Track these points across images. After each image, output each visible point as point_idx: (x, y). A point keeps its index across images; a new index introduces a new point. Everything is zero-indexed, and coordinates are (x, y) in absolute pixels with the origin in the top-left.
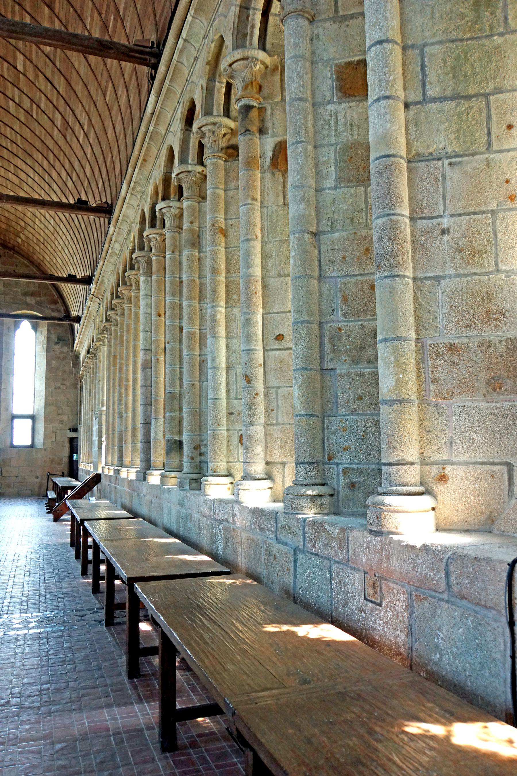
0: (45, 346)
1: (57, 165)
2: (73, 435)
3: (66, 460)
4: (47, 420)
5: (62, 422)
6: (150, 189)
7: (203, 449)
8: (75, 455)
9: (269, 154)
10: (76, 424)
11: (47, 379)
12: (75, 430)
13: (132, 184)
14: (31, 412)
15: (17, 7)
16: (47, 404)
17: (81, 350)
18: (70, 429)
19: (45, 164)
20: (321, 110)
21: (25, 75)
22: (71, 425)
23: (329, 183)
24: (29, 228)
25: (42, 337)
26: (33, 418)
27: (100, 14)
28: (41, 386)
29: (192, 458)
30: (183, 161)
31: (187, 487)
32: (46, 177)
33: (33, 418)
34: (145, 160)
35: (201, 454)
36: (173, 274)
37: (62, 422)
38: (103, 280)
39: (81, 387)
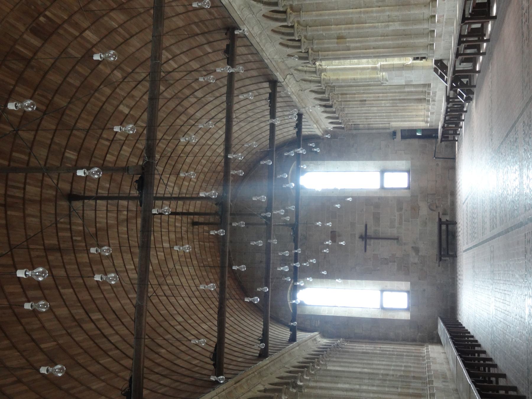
0: (319, 162)
1: (186, 103)
2: (399, 135)
3: (422, 142)
4: (385, 157)
8: (418, 134)
11: (349, 160)
12: (394, 133)
14: (378, 174)
15: (96, 94)
16: (371, 159)
17: (323, 126)
18: (394, 139)
19: (184, 118)
21: (131, 109)
25: (312, 165)
26: (383, 172)
27: (113, 9)
28: (354, 165)
32: (192, 122)
33: (383, 172)
39: (356, 127)
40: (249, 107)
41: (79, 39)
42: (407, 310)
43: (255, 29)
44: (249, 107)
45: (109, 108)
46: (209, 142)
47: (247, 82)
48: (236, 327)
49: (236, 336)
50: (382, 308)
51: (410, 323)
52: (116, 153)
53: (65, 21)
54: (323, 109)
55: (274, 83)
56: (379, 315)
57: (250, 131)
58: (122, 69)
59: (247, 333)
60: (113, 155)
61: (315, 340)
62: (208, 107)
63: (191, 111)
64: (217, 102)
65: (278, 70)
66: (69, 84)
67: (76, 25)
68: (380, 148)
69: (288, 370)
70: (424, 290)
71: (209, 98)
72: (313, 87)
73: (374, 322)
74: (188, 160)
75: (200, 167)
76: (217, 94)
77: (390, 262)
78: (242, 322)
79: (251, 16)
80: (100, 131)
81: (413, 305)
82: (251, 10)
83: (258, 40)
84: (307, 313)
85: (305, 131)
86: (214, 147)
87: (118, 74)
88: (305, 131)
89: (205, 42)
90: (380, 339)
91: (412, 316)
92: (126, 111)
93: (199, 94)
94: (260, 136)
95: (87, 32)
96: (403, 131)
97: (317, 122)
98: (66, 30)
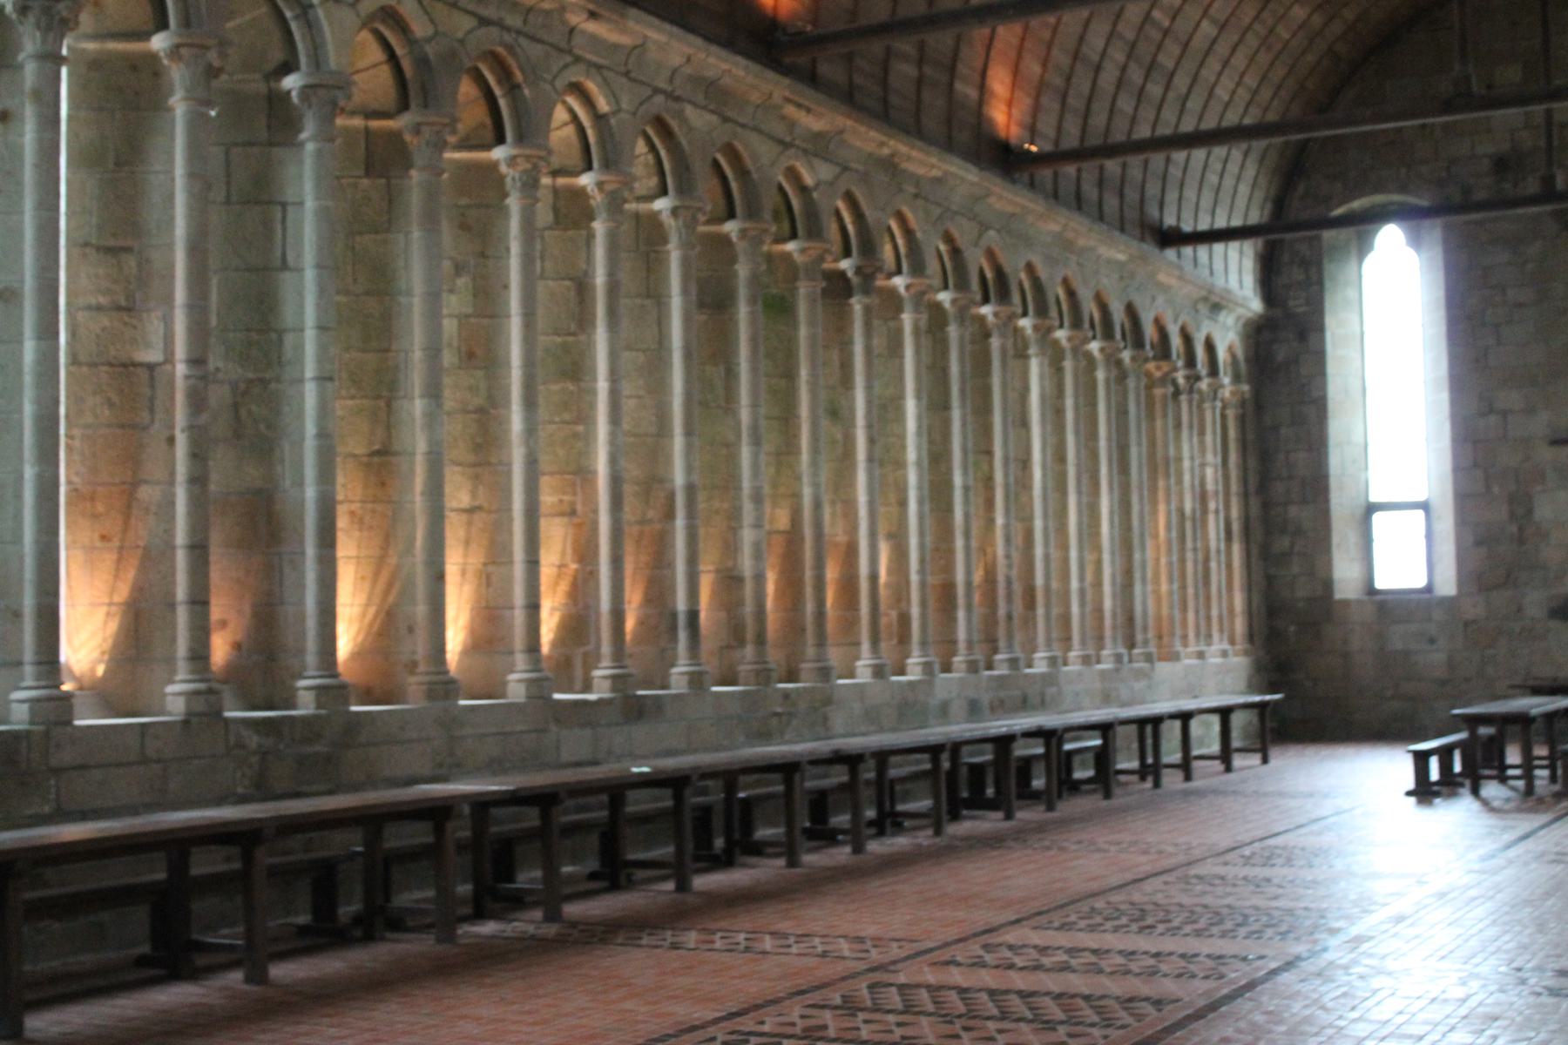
42: (1371, 591)
48: (1172, 49)
49: (1118, 54)
50: (1371, 509)
51: (1323, 601)
56: (1341, 503)
59: (1154, 89)
61: (1216, 308)
69: (962, 241)
70: (1432, 641)
73: (1316, 486)
77: (1520, 529)
78: (1214, 65)
81: (1388, 607)
84: (1329, 268)
90: (1266, 506)
91: (1345, 603)
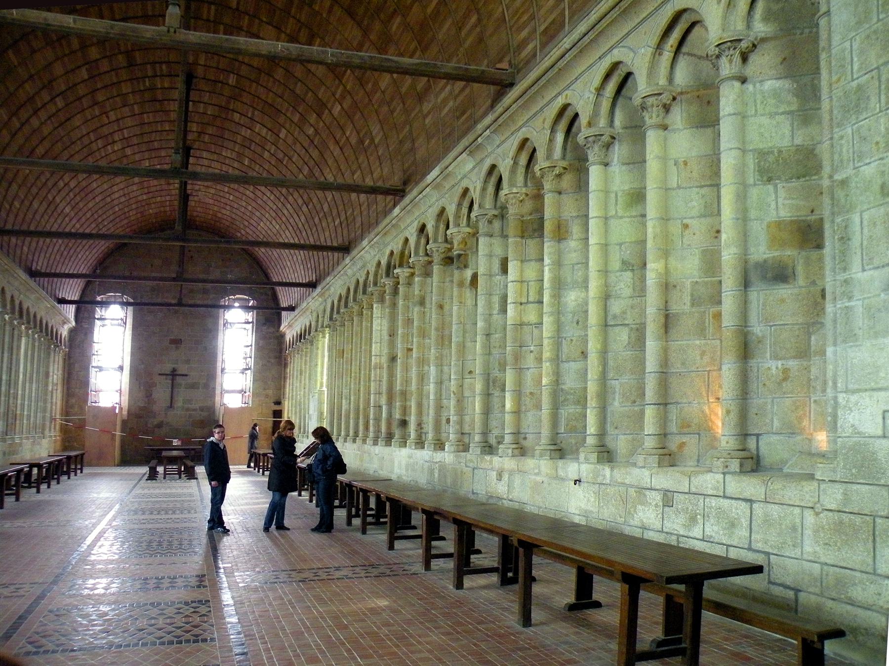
2: (277, 408)
5: (267, 396)
6: (388, 252)
7: (423, 426)
9: (469, 279)
10: (280, 398)
12: (278, 403)
13: (372, 243)
15: (291, 108)
17: (288, 332)
20: (493, 278)
22: (273, 400)
23: (495, 312)
24: (252, 227)
29: (416, 431)
30: (416, 253)
31: (414, 447)
34: (385, 234)
35: (421, 428)
36: (403, 314)
37: (267, 396)
38: (329, 287)
39: (286, 365)
40: (299, 258)
41: (333, 98)
43: (349, 270)
44: (299, 258)
45: (281, 120)
46: (267, 215)
47: (316, 259)
52: (242, 122)
53: (345, 87)
54: (299, 332)
55: (312, 285)
57: (282, 257)
58: (315, 135)
60: (240, 119)
62: (295, 216)
63: (290, 198)
64: (300, 226)
65: (323, 291)
66: (296, 84)
67: (343, 97)
68: (265, 389)
71: (303, 218)
72: (313, 324)
74: (248, 192)
75: (244, 204)
76: (306, 226)
79: (358, 267)
80: (259, 108)
82: (362, 268)
83: (342, 272)
85: (284, 313)
86: (264, 219)
87: (311, 131)
88: (284, 313)
89: (342, 220)
92: (282, 135)
93: (304, 208)
94: (279, 267)
95: (339, 107)
96: (281, 411)
97: (290, 326)
98: (338, 87)
